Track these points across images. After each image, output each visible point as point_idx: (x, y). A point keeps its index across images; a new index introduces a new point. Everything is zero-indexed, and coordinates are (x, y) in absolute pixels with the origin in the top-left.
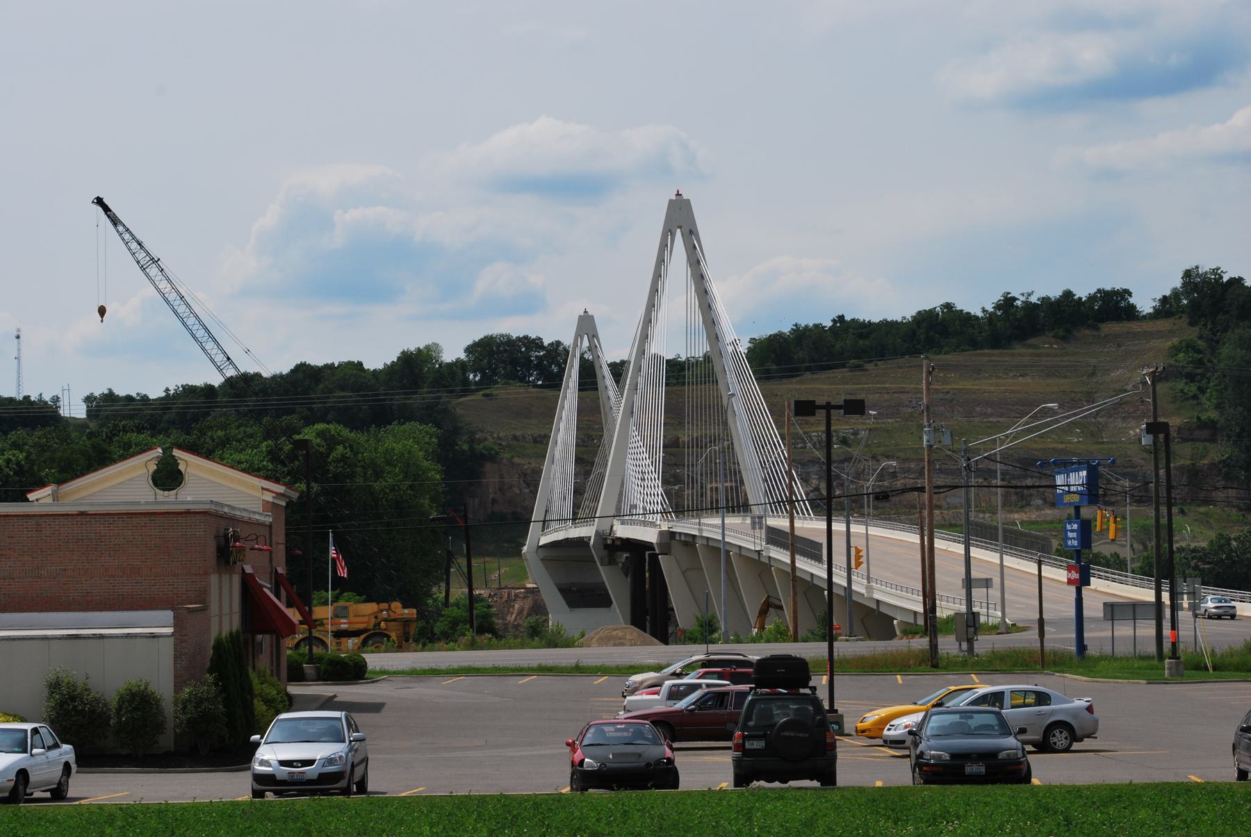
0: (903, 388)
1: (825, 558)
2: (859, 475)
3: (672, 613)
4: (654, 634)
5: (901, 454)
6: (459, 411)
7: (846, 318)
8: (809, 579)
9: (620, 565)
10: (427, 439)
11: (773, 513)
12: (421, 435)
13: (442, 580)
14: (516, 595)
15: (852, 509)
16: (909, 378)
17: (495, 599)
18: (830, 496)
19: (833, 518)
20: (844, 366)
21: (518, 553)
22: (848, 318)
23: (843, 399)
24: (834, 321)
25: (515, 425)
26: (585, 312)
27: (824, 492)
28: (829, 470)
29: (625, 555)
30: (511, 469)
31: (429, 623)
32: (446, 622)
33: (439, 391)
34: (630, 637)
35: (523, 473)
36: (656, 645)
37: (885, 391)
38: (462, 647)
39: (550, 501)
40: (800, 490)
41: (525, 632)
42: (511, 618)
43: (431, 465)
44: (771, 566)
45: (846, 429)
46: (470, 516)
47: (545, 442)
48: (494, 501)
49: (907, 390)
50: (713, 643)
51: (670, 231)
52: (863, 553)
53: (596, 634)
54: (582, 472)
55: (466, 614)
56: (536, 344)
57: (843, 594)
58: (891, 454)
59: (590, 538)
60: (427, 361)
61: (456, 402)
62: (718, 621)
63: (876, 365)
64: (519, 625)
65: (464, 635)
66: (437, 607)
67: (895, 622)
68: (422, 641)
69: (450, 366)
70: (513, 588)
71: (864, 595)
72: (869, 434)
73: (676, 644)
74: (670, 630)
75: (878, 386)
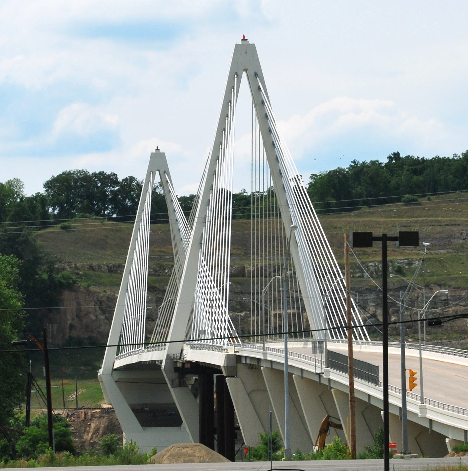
0: (455, 221)
1: (381, 380)
2: (413, 303)
3: (238, 431)
4: (221, 452)
5: (453, 283)
6: (39, 242)
7: (401, 156)
8: (366, 400)
9: (190, 387)
10: (9, 269)
11: (333, 338)
12: (3, 265)
13: (23, 401)
14: (93, 415)
15: (407, 334)
16: (460, 211)
17: (73, 418)
18: (386, 323)
19: (389, 343)
20: (399, 200)
21: (94, 376)
22: (403, 155)
23: (398, 231)
24: (390, 158)
25: (92, 255)
26: (157, 149)
27: (381, 319)
28: (385, 298)
29: (194, 378)
30: (87, 297)
31: (11, 441)
32: (27, 441)
33: (20, 224)
34: (199, 455)
35: (98, 301)
36: (223, 461)
37: (437, 224)
38: (41, 463)
39: (124, 327)
40: (358, 317)
41: (100, 449)
42: (87, 437)
43: (12, 293)
44: (331, 388)
45: (401, 259)
46: (50, 340)
47: (119, 272)
48: (72, 327)
49: (458, 223)
50: (276, 460)
51: (237, 74)
52: (417, 376)
53: (168, 451)
54: (154, 299)
55: (46, 433)
56: (111, 179)
57: (398, 414)
58: (442, 282)
59: (161, 362)
60: (8, 196)
61: (36, 234)
62: (282, 440)
63: (429, 199)
64: (95, 443)
65: (44, 452)
66: (18, 426)
67: (447, 440)
68: (4, 458)
69: (31, 200)
70: (90, 409)
71: (418, 415)
72: (423, 264)
73: (242, 461)
74: (237, 448)
75: (431, 219)
